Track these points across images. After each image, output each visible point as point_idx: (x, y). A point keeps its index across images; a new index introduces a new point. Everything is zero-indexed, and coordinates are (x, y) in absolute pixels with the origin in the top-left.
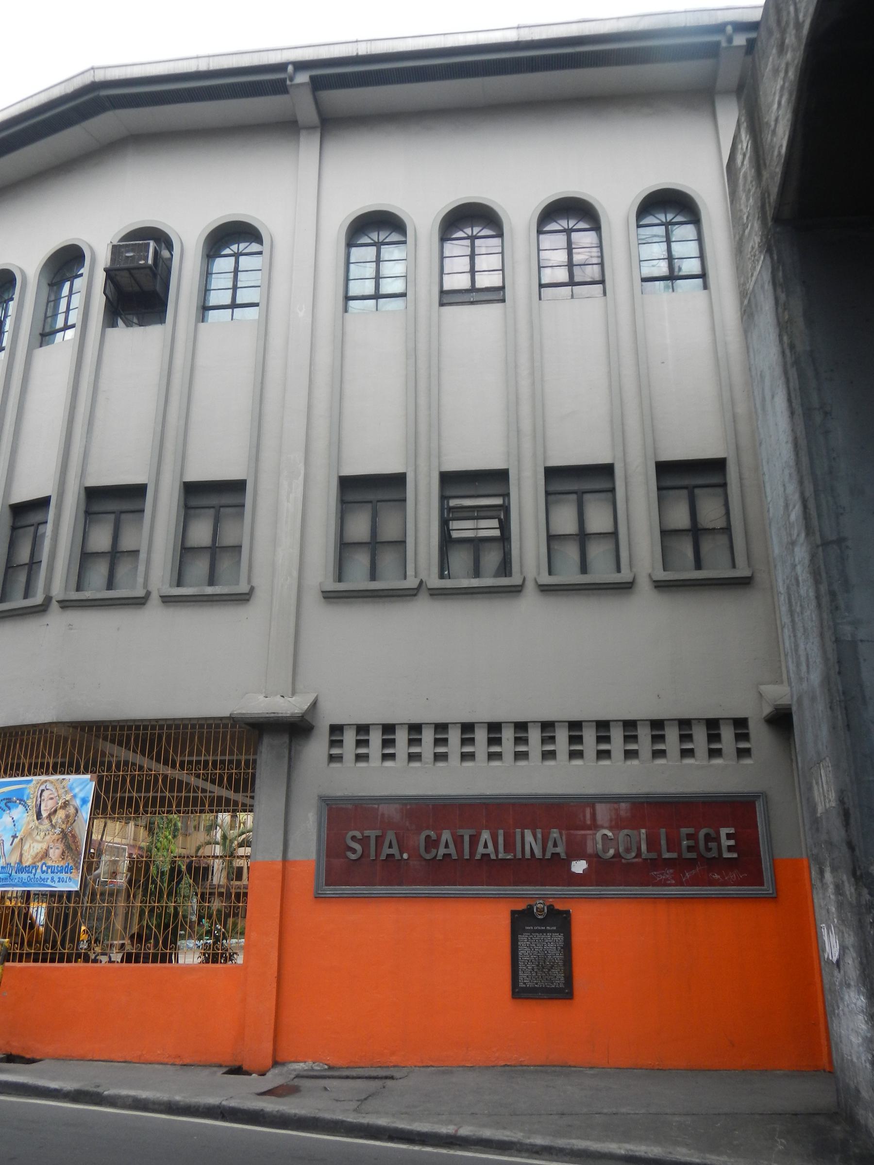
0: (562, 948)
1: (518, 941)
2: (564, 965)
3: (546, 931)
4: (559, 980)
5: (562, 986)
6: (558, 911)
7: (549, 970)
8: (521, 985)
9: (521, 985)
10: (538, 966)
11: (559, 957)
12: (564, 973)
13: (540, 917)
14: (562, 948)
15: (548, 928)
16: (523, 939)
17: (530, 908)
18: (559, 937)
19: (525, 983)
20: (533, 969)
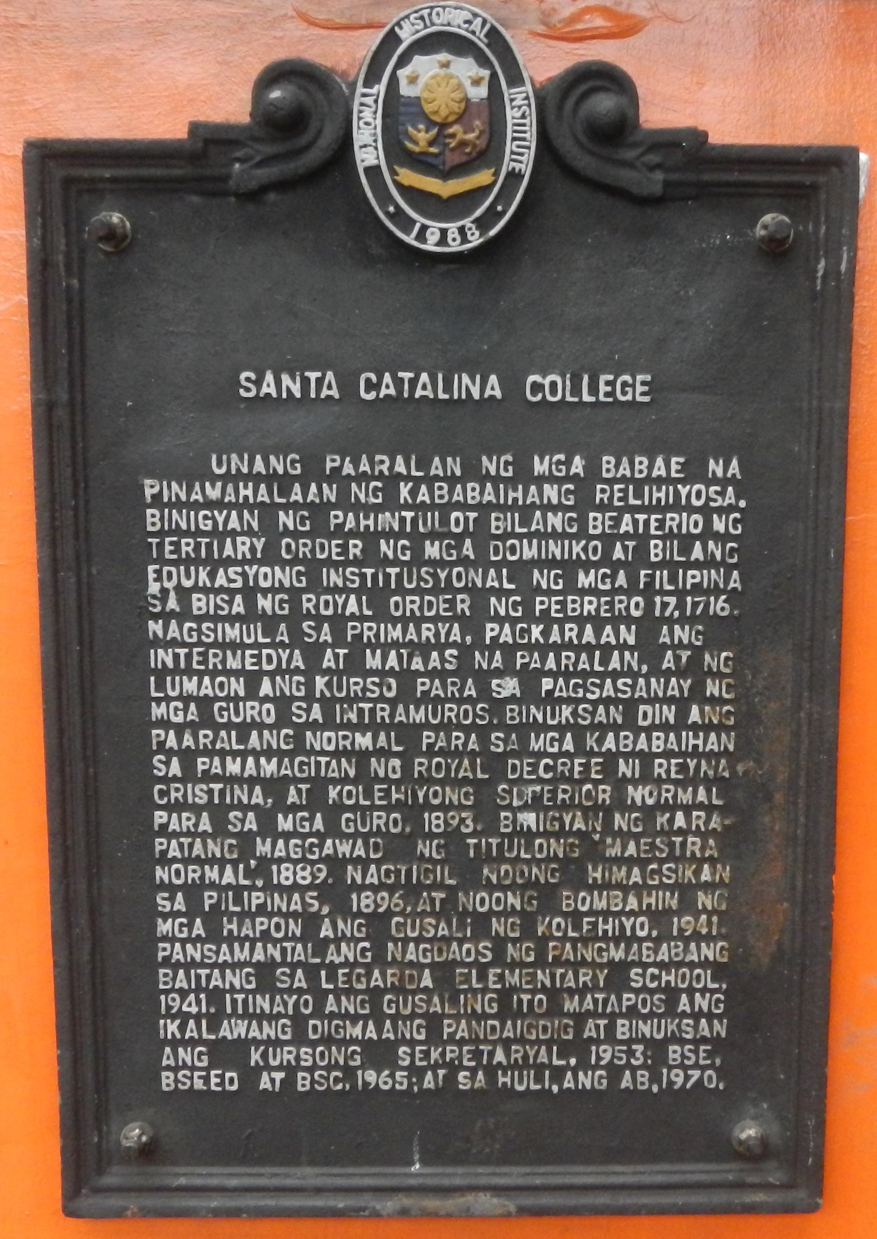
0: (716, 632)
1: (136, 552)
2: (735, 842)
3: (521, 427)
4: (665, 1024)
5: (689, 1070)
6: (687, 150)
7: (547, 898)
8: (185, 1070)
9: (185, 1070)
10: (399, 848)
11: (671, 743)
12: (732, 923)
13: (435, 236)
14: (716, 632)
15: (549, 384)
16: (212, 546)
17: (298, 112)
18: (696, 505)
19: (225, 1053)
20: (336, 892)
